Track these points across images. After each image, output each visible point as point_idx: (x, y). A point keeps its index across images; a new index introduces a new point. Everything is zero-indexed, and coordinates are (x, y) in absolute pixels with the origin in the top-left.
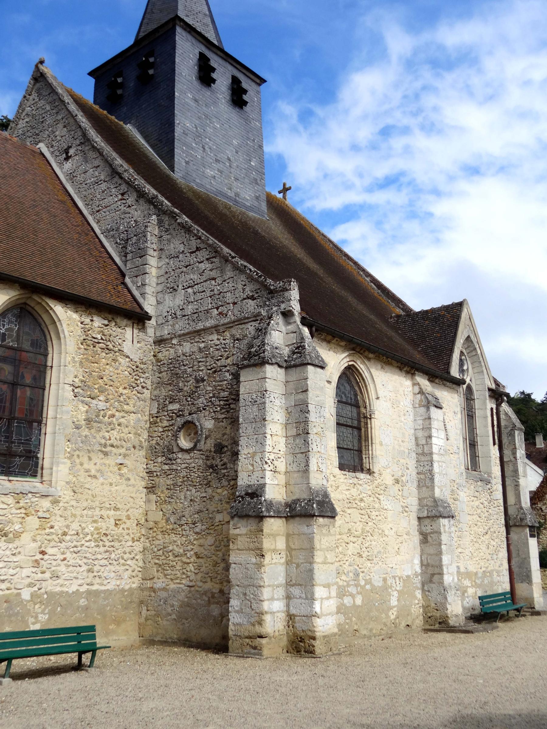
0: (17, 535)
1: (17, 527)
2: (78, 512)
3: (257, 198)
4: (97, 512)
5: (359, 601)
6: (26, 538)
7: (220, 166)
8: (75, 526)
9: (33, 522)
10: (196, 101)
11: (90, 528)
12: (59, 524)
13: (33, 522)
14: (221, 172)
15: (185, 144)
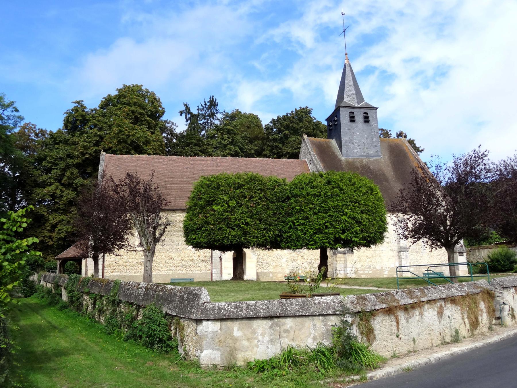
0: (297, 260)
1: (296, 258)
2: (310, 255)
3: (377, 151)
4: (315, 255)
5: (370, 272)
6: (299, 261)
7: (360, 147)
8: (309, 258)
9: (300, 258)
10: (349, 129)
11: (313, 258)
12: (306, 258)
13: (300, 258)
14: (361, 149)
15: (346, 145)
